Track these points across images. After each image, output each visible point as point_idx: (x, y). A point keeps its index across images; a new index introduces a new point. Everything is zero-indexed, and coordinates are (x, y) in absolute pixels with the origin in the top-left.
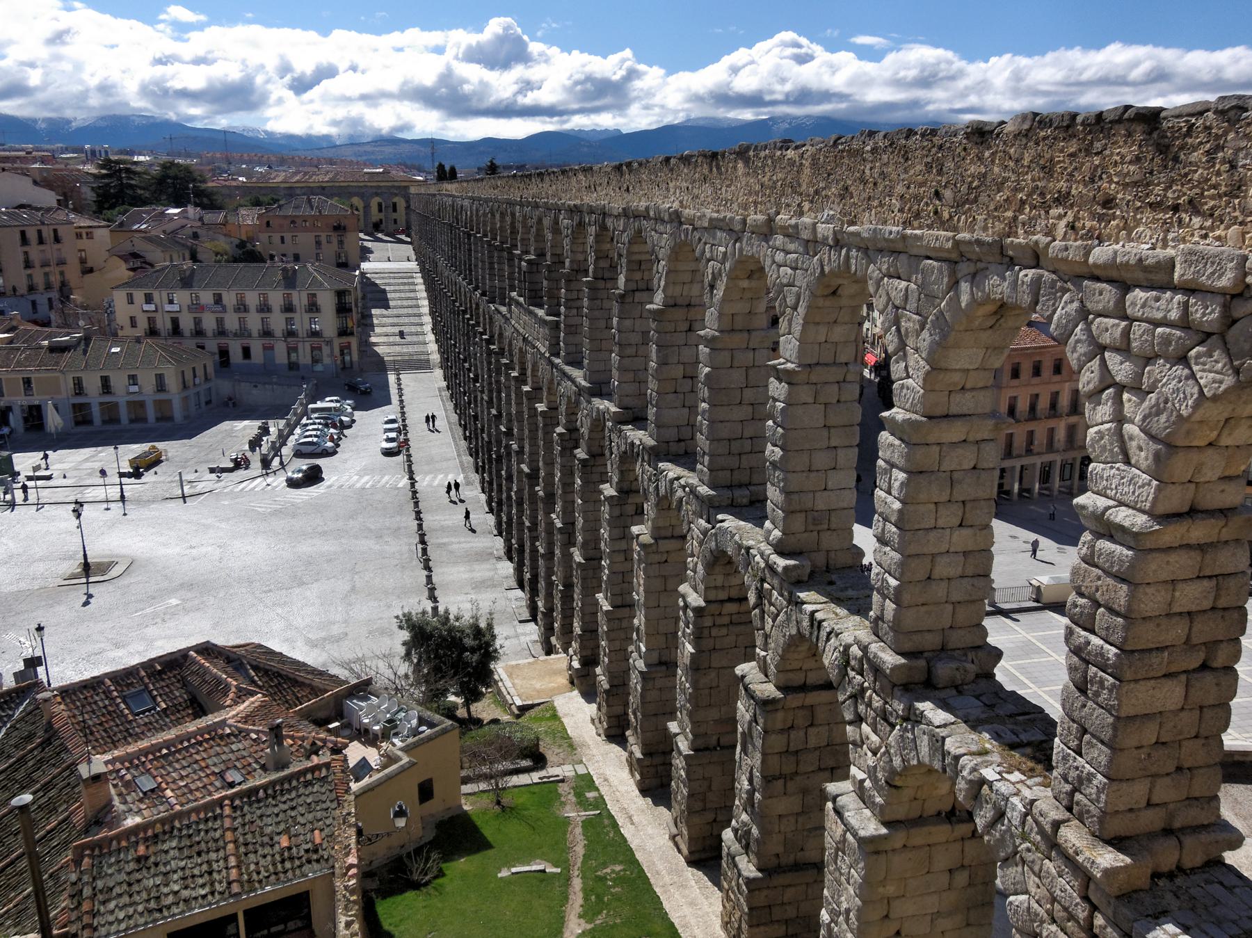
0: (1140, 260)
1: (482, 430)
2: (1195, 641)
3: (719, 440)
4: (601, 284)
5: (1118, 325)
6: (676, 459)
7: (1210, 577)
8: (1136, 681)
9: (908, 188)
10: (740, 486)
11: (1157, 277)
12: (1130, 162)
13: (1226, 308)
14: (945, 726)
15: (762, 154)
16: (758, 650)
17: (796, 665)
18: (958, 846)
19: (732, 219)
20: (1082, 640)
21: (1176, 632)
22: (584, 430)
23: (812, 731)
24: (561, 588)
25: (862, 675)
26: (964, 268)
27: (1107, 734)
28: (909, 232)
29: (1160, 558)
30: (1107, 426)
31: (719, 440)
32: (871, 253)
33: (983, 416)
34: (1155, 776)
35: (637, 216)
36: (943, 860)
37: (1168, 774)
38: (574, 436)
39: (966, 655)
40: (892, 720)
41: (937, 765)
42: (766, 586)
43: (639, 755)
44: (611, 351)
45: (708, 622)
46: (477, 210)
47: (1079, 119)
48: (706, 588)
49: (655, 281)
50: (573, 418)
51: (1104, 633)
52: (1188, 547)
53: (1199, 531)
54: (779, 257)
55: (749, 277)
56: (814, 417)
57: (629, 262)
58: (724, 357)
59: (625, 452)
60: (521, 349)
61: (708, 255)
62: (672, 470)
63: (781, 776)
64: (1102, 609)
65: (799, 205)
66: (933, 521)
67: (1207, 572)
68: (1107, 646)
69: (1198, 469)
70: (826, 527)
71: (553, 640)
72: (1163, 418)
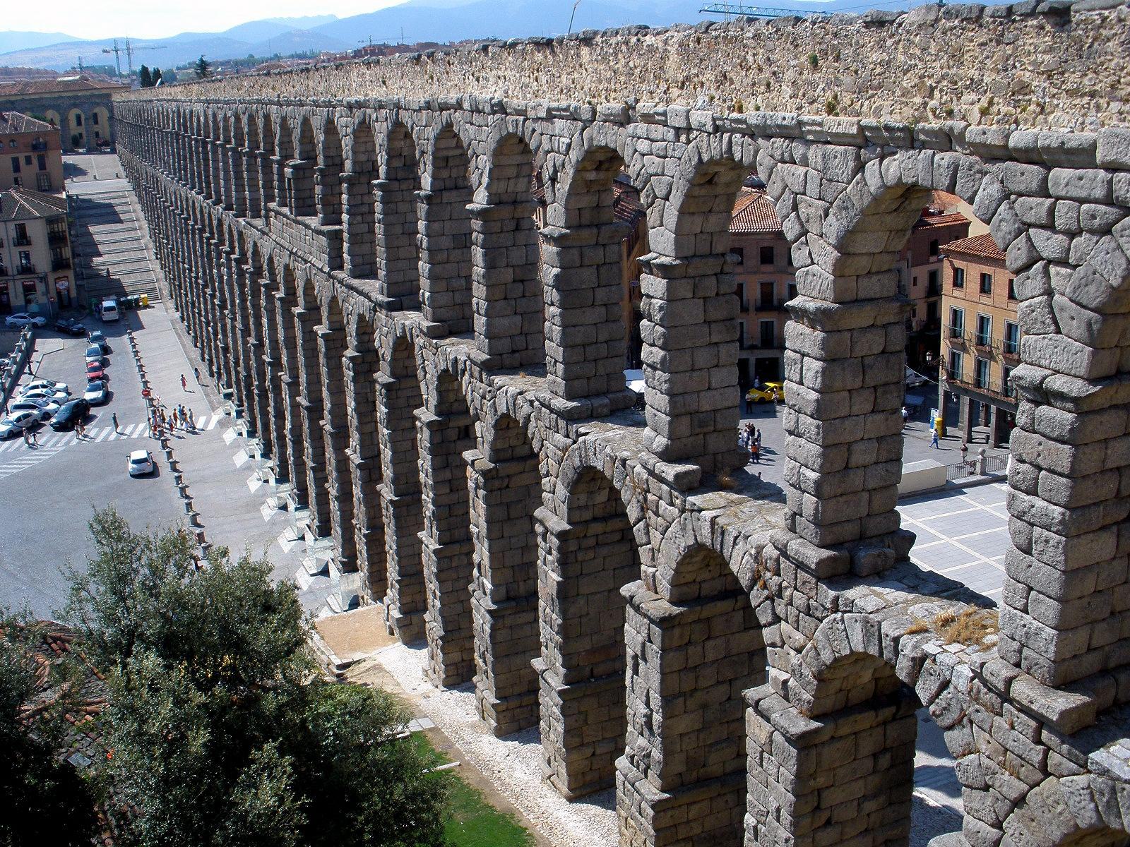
0: (1063, 143)
1: (237, 363)
4: (395, 185)
5: (1042, 204)
6: (512, 370)
8: (1078, 536)
10: (598, 394)
11: (1081, 157)
12: (1044, 52)
14: (877, 611)
15: (613, 41)
16: (643, 567)
17: (689, 578)
18: (880, 730)
20: (1026, 505)
22: (386, 351)
23: (710, 644)
24: (364, 531)
25: (779, 575)
27: (1055, 589)
30: (1037, 300)
33: (889, 299)
35: (443, 107)
36: (867, 746)
38: (369, 358)
39: (882, 541)
40: (818, 614)
41: (873, 650)
42: (650, 496)
44: (418, 259)
45: (573, 546)
46: (215, 115)
47: (988, 11)
48: (570, 509)
50: (366, 338)
51: (1047, 495)
54: (643, 146)
55: (598, 169)
56: (693, 312)
57: (434, 158)
59: (446, 371)
60: (287, 267)
61: (546, 146)
63: (681, 694)
64: (1043, 472)
65: (665, 93)
70: (712, 428)
72: (1092, 288)
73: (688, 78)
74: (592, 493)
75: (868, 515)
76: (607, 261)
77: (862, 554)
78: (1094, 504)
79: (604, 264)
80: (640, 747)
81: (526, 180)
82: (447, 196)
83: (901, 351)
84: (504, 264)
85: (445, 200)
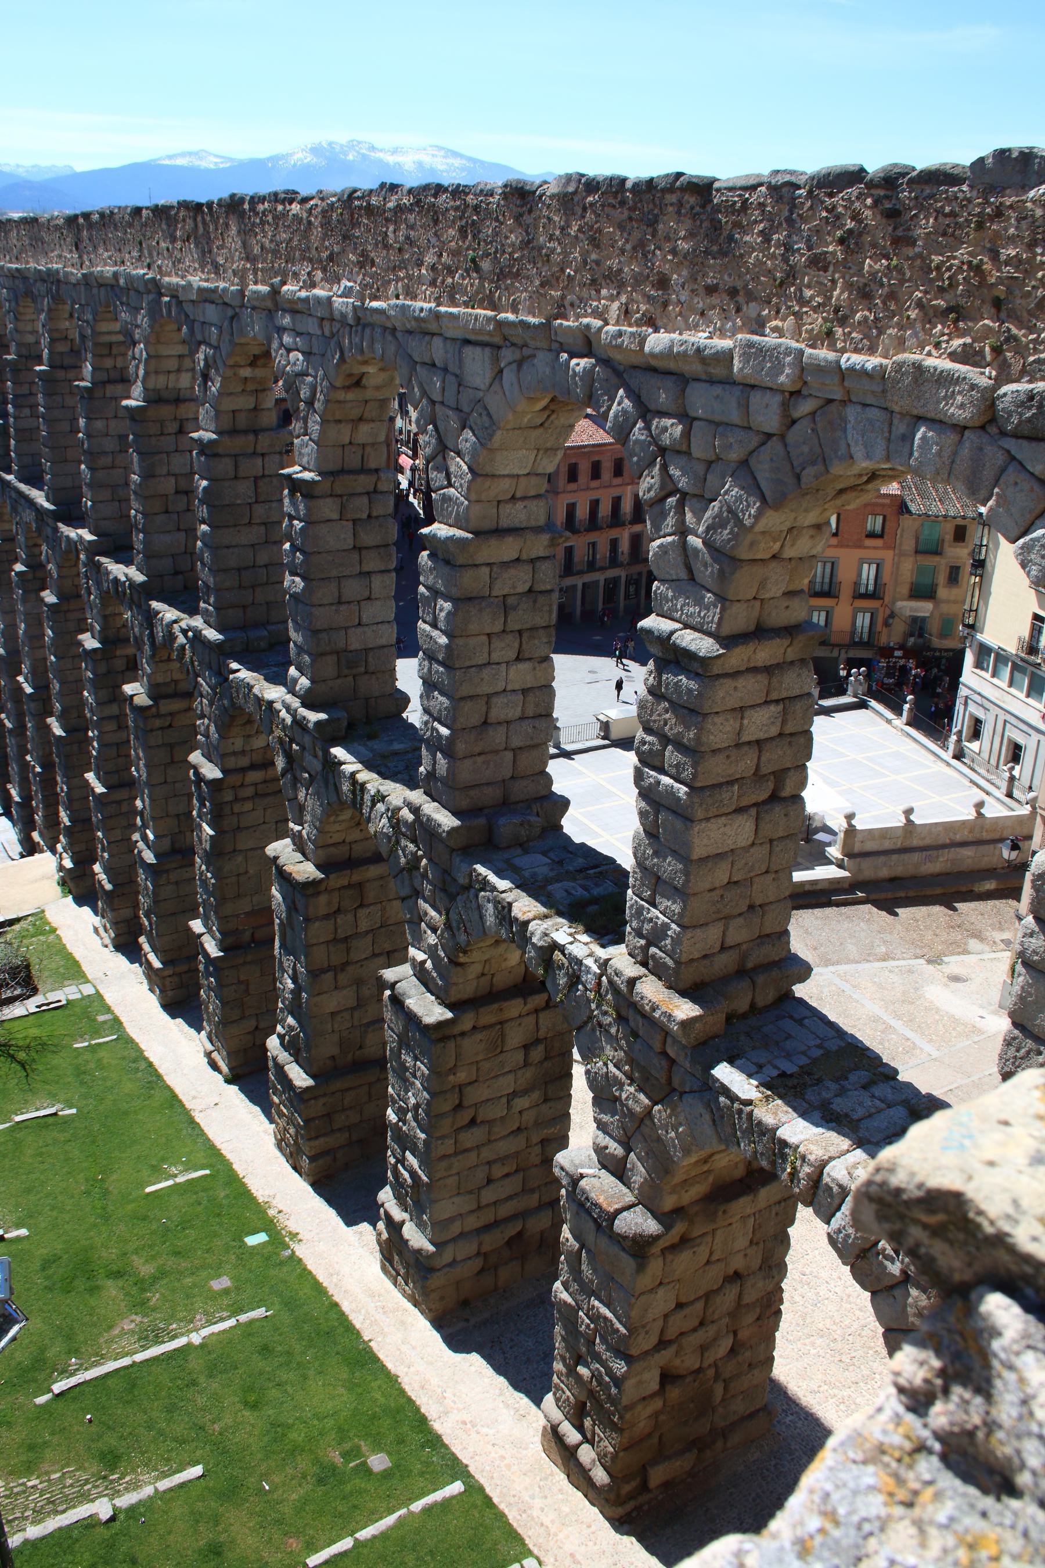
2: (764, 770)
3: (225, 571)
4: (61, 374)
7: (777, 702)
8: (708, 819)
9: (441, 255)
13: (785, 406)
15: (261, 207)
17: (337, 838)
18: (531, 1019)
19: (225, 290)
21: (745, 764)
24: (38, 769)
26: (508, 355)
28: (443, 309)
29: (728, 683)
30: (669, 539)
31: (225, 571)
32: (399, 335)
33: (537, 530)
34: (728, 918)
36: (516, 1037)
37: (740, 915)
43: (157, 964)
44: (80, 462)
45: (228, 796)
49: (132, 370)
50: (36, 551)
52: (754, 670)
53: (764, 653)
56: (339, 537)
57: (95, 344)
58: (225, 466)
61: (199, 337)
62: (169, 614)
63: (329, 969)
65: (309, 274)
66: (486, 655)
67: (774, 696)
68: (677, 785)
69: (763, 584)
70: (363, 669)
71: (36, 836)
73: (331, 258)
74: (249, 736)
75: (512, 777)
76: (267, 473)
77: (502, 821)
78: (728, 783)
79: (264, 476)
80: (290, 1026)
81: (190, 374)
82: (111, 390)
83: (551, 591)
84: (164, 471)
85: (108, 395)
